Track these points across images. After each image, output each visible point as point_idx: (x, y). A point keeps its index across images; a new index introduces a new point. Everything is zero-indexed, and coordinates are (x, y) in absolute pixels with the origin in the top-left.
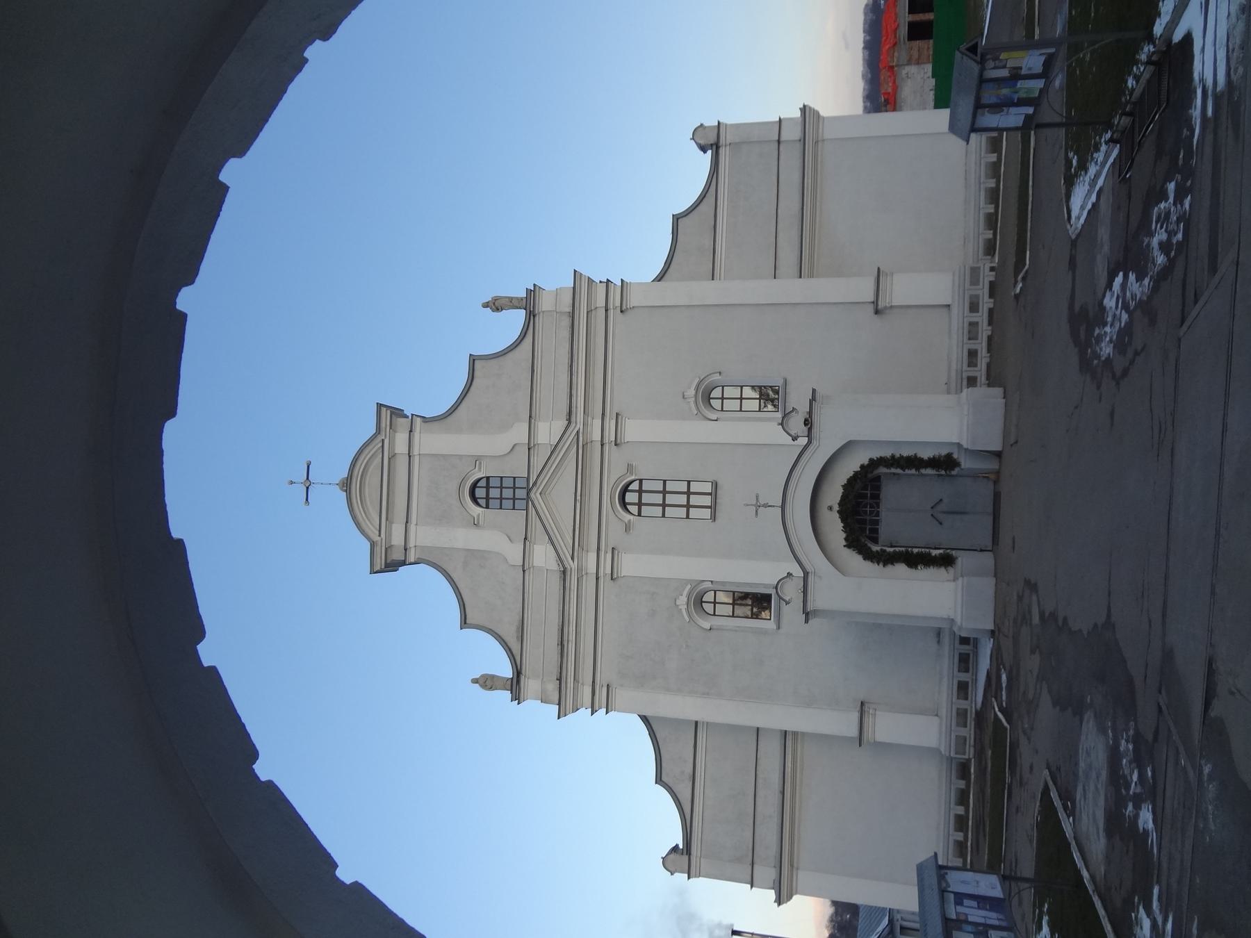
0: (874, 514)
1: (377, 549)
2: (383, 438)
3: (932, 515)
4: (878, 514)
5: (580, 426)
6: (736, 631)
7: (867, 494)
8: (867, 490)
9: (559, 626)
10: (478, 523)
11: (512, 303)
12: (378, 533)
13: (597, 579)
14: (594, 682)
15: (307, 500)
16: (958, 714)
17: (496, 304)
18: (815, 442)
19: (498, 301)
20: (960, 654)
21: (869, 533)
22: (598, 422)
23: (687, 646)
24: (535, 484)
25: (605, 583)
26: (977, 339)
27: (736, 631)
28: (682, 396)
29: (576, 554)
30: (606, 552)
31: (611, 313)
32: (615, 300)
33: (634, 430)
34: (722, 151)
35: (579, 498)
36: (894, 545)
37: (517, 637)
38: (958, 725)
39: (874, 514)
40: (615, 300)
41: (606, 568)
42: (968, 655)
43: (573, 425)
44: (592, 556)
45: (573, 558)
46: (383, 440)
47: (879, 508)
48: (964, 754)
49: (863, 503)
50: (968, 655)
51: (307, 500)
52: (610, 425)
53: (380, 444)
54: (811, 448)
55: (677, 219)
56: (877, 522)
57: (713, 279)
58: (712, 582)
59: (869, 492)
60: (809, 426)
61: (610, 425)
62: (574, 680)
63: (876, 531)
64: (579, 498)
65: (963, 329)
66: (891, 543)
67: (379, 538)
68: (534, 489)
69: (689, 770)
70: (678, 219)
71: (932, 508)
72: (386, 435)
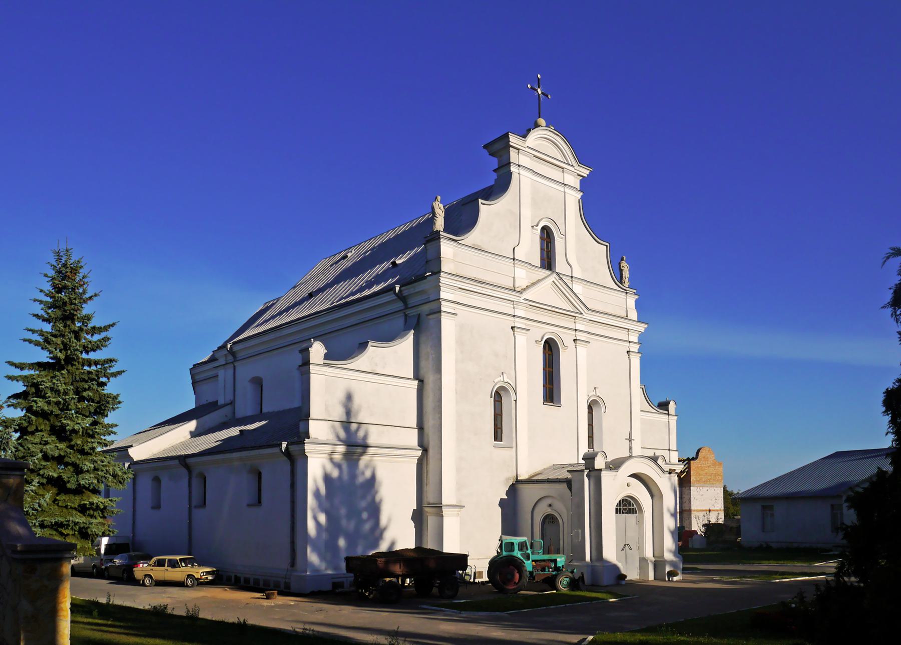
4: (623, 513)
5: (586, 316)
23: (481, 379)
24: (561, 279)
25: (510, 322)
29: (527, 302)
33: (582, 350)
37: (474, 245)
41: (519, 323)
45: (525, 299)
46: (572, 166)
47: (626, 513)
53: (571, 164)
57: (641, 411)
62: (460, 288)
64: (554, 309)
65: (337, 578)
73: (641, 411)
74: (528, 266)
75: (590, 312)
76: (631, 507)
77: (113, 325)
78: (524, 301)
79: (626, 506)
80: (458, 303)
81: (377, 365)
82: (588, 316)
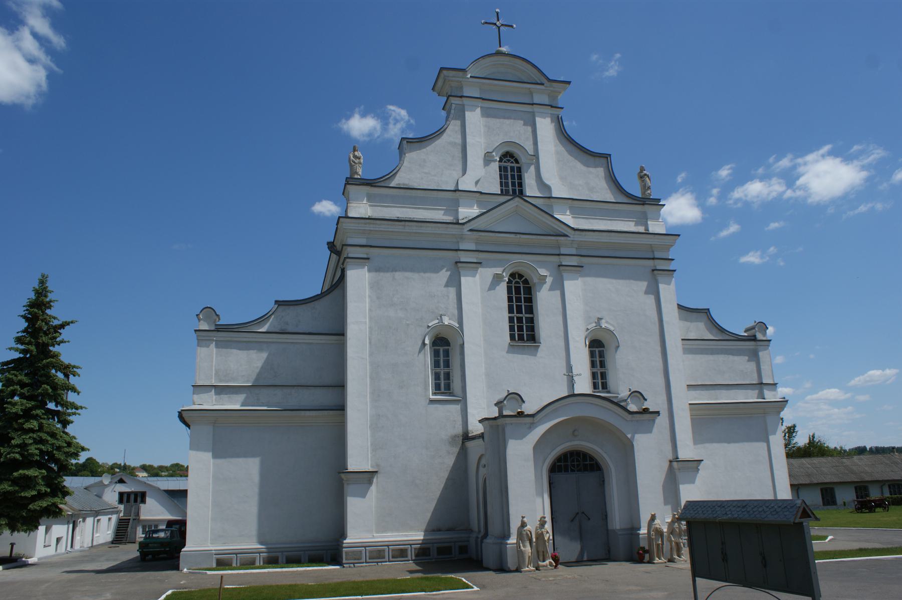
0: (572, 468)
1: (461, 73)
2: (545, 85)
3: (578, 513)
4: (572, 471)
6: (425, 365)
7: (587, 461)
8: (590, 461)
9: (414, 218)
10: (488, 156)
11: (645, 188)
12: (473, 75)
13: (456, 250)
14: (371, 246)
15: (486, 23)
16: (380, 551)
17: (646, 176)
18: (630, 416)
19: (647, 179)
20: (429, 549)
21: (558, 465)
22: (574, 252)
23: (408, 325)
27: (425, 365)
28: (600, 317)
30: (477, 258)
31: (650, 263)
32: (661, 265)
34: (752, 343)
35: (518, 236)
36: (552, 485)
37: (399, 184)
38: (371, 552)
39: (572, 468)
40: (661, 265)
41: (464, 257)
42: (430, 556)
43: (573, 232)
44: (472, 247)
45: (471, 230)
47: (578, 471)
48: (346, 560)
49: (579, 459)
50: (430, 556)
51: (486, 23)
52: (574, 261)
53: (539, 82)
54: (626, 414)
55: (707, 311)
56: (566, 470)
58: (464, 344)
60: (643, 412)
61: (574, 261)
63: (560, 470)
66: (553, 483)
67: (469, 76)
69: (290, 329)
70: (706, 312)
71: (583, 513)
72: (546, 87)
73: (682, 340)
74: (478, 195)
75: (577, 233)
76: (588, 462)
77: (72, 322)
78: (469, 233)
79: (578, 461)
80: (371, 246)
81: (287, 324)
82: (578, 237)
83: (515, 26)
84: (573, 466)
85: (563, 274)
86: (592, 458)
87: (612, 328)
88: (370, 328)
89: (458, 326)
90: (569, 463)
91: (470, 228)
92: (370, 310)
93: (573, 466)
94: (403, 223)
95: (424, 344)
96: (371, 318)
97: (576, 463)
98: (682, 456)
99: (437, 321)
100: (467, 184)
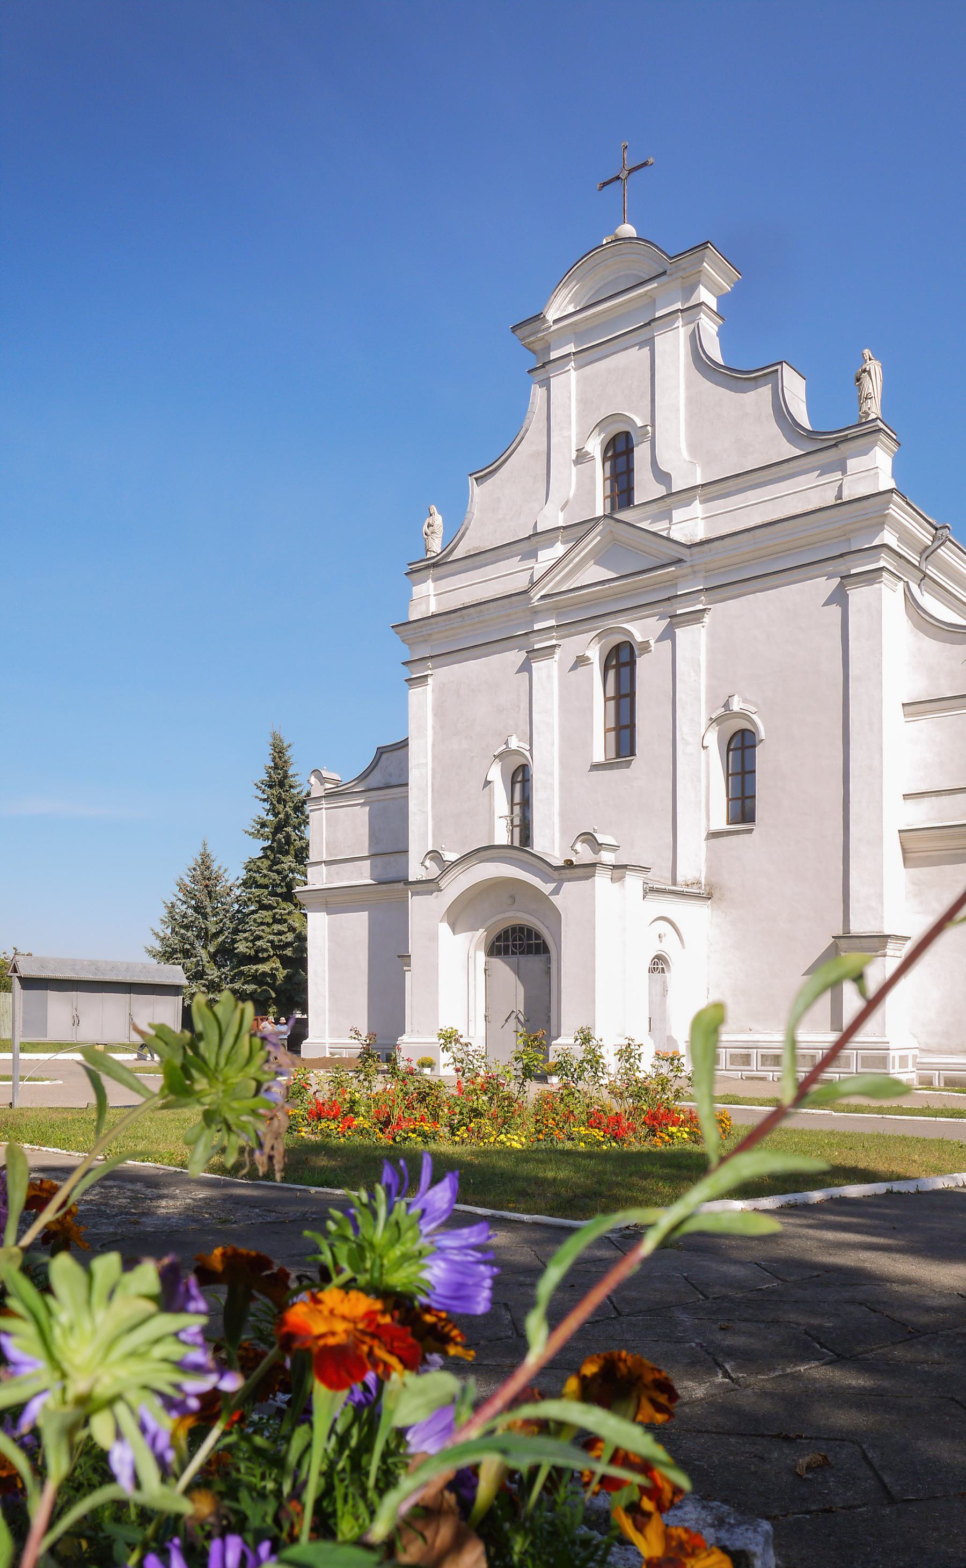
4: (514, 953)
9: (481, 599)
10: (581, 457)
15: (605, 184)
26: (763, 1065)
45: (543, 597)
51: (605, 184)
59: (533, 941)
68: (612, 522)
81: (391, 776)
83: (651, 160)
84: (515, 946)
85: (676, 630)
86: (538, 936)
87: (754, 709)
88: (433, 769)
89: (528, 748)
90: (510, 943)
91: (542, 593)
92: (433, 745)
93: (515, 946)
94: (459, 613)
95: (487, 783)
96: (434, 757)
97: (518, 943)
98: (857, 927)
99: (505, 746)
100: (551, 517)
